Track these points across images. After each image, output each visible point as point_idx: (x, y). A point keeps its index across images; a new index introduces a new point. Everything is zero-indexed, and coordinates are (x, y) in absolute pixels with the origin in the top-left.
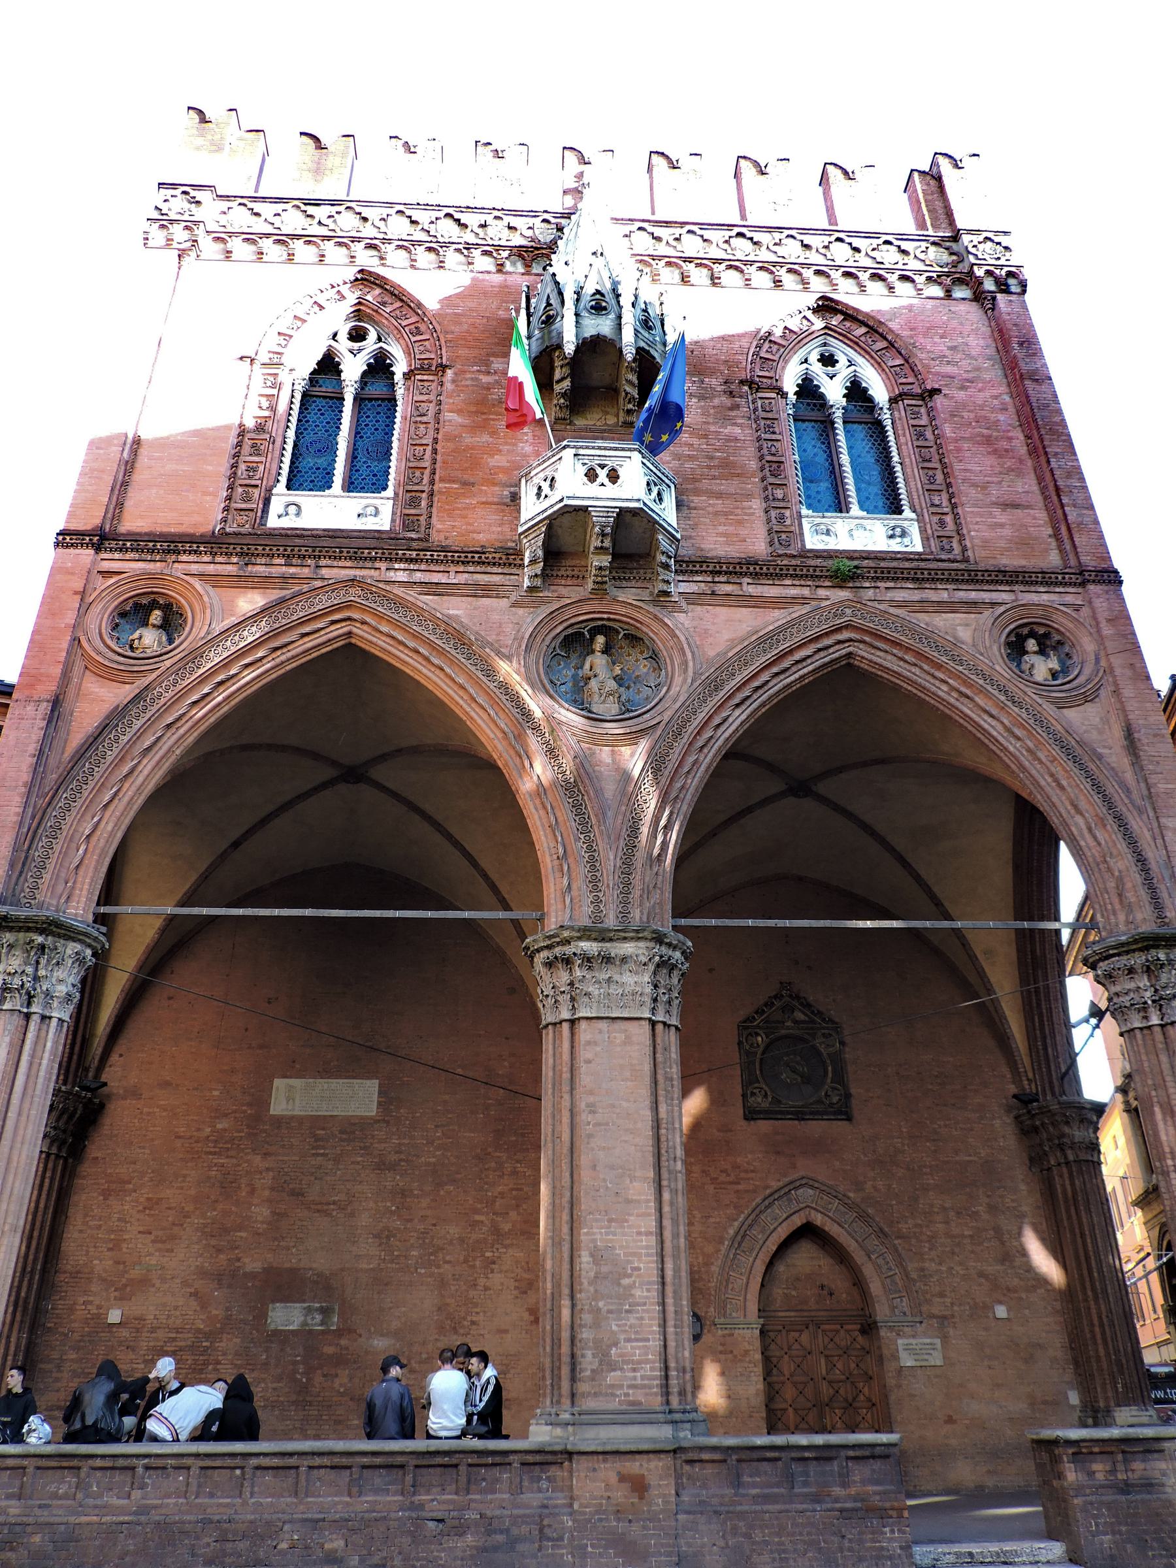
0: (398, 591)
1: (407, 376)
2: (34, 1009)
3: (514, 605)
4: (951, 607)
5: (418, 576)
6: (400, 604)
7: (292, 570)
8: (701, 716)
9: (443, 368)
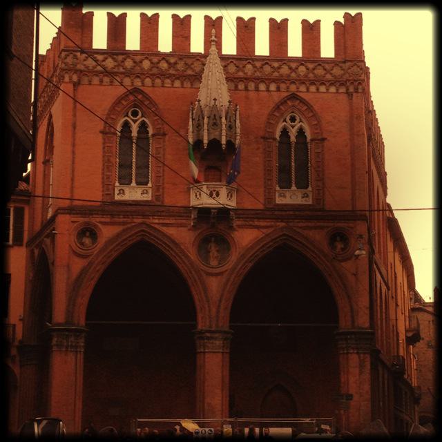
0: (156, 226)
1: (153, 135)
2: (78, 350)
3: (189, 230)
4: (315, 228)
5: (161, 221)
6: (155, 229)
7: (125, 219)
8: (240, 266)
9: (164, 135)
